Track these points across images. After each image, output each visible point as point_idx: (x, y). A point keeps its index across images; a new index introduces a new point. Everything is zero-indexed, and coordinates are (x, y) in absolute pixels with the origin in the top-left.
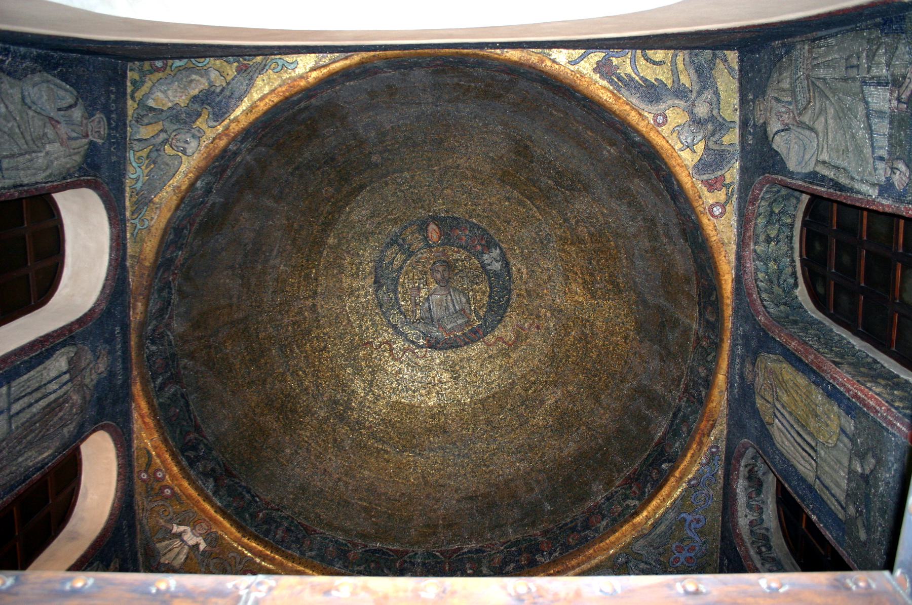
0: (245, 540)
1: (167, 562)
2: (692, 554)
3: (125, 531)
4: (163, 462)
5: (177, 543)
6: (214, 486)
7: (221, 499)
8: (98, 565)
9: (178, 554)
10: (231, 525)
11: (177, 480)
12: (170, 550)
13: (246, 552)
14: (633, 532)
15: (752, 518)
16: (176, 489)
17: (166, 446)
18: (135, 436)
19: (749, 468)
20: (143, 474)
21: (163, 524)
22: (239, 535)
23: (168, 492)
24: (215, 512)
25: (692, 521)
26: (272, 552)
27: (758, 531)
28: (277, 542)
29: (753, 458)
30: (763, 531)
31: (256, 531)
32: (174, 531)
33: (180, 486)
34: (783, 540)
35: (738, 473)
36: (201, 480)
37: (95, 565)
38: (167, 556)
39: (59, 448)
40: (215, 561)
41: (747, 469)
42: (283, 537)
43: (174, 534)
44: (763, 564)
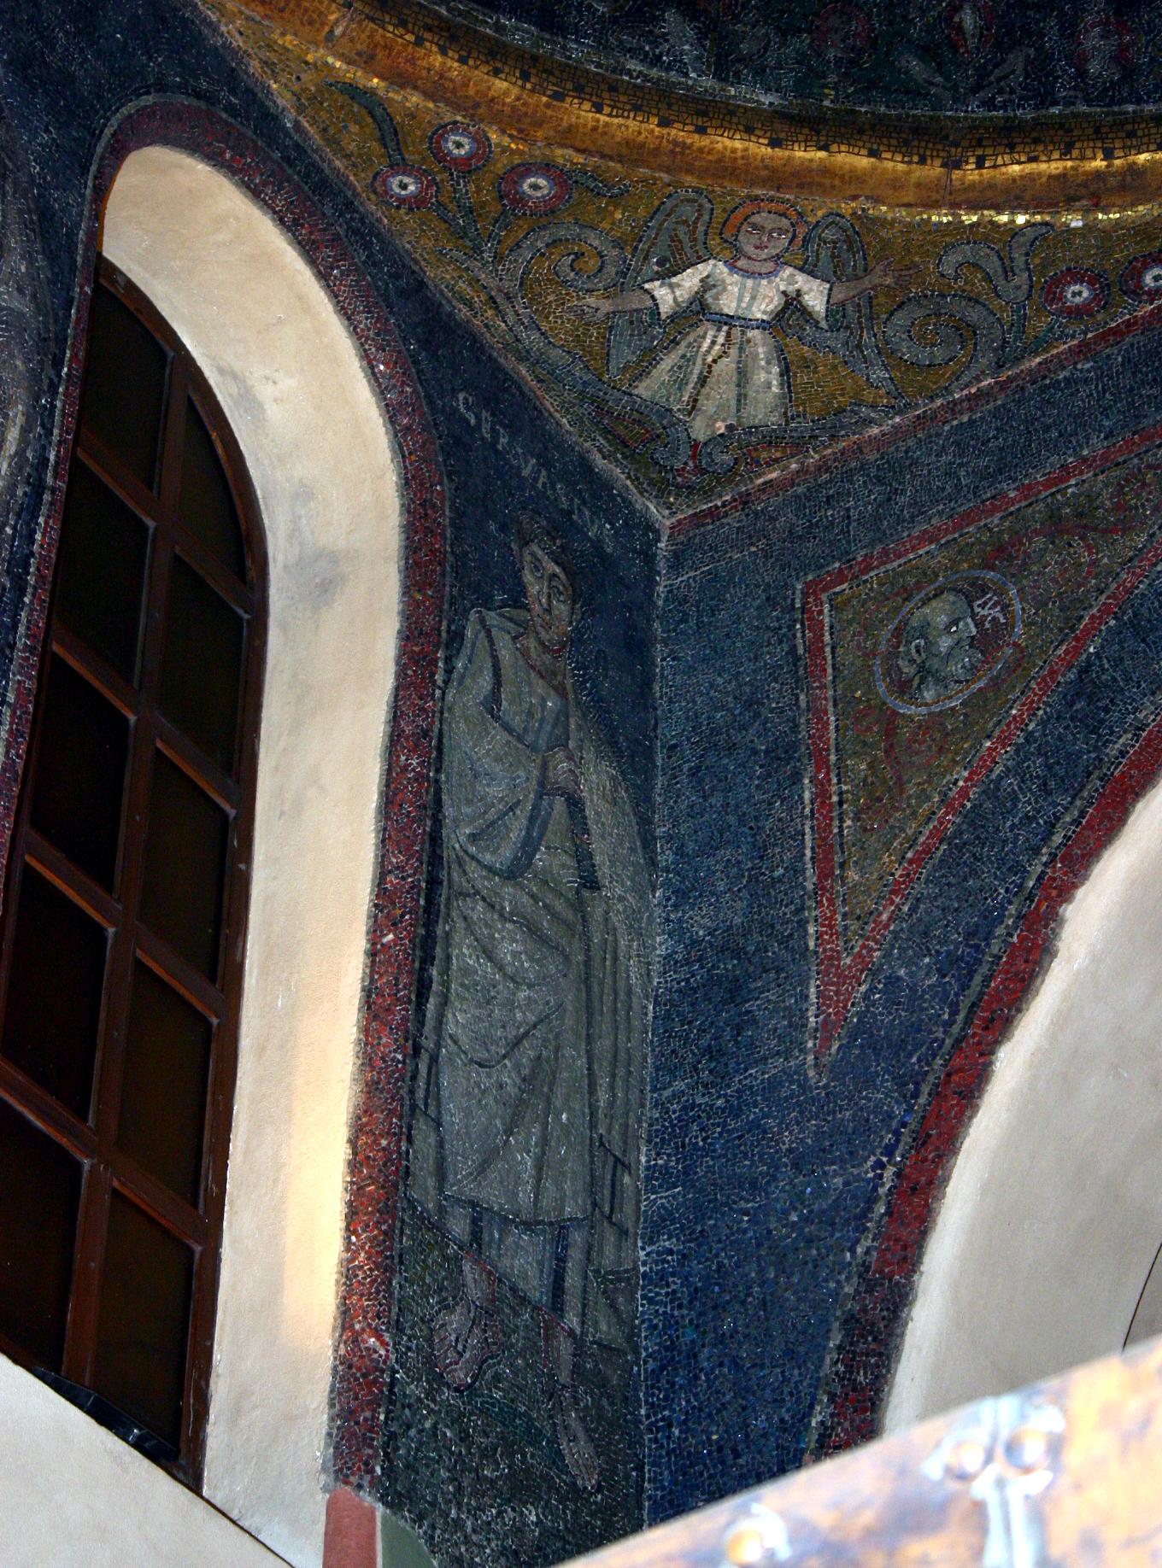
0: (970, 174)
1: (721, 427)
3: (485, 431)
4: (437, 90)
5: (710, 340)
6: (702, 35)
7: (760, 72)
8: (482, 621)
9: (743, 375)
10: (872, 154)
11: (539, 124)
12: (703, 381)
13: (1004, 218)
16: (561, 155)
17: (402, 23)
18: (254, 66)
20: (394, 182)
21: (606, 306)
22: (933, 171)
23: (537, 186)
24: (774, 143)
26: (1108, 155)
28: (1108, 95)
31: (989, 104)
32: (666, 308)
33: (567, 136)
36: (633, 52)
37: (469, 633)
38: (708, 406)
39: (34, 377)
40: (900, 319)
42: (1120, 58)
43: (673, 317)
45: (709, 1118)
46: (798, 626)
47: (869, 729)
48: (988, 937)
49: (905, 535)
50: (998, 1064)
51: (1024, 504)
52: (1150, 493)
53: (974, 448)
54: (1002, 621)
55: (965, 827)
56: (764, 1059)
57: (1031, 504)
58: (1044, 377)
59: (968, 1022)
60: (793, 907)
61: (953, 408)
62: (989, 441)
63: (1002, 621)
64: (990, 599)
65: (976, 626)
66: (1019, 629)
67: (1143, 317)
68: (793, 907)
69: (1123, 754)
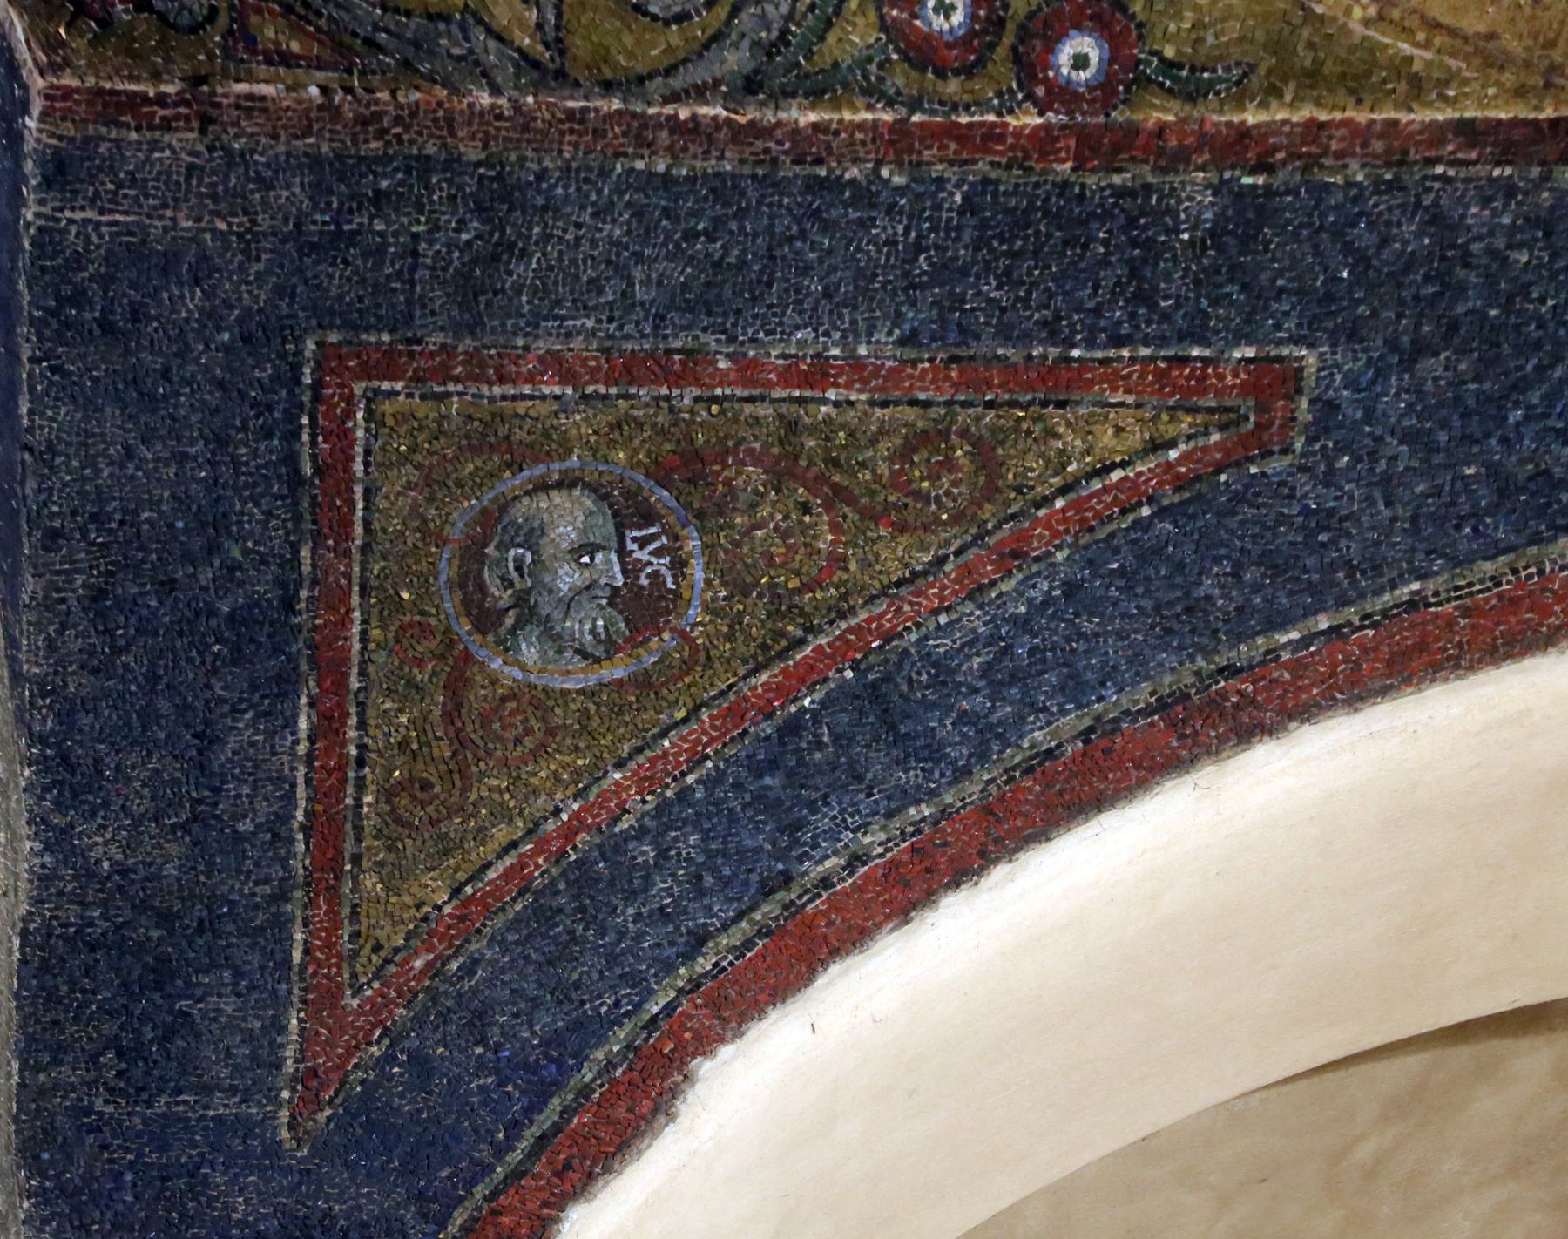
45: (114, 1137)
46: (305, 420)
47: (420, 663)
48: (580, 1057)
49: (520, 342)
50: (567, 1225)
51: (739, 392)
52: (955, 484)
53: (668, 238)
54: (671, 586)
55: (562, 886)
56: (207, 1089)
57: (751, 400)
58: (819, 161)
59: (533, 1154)
60: (267, 889)
61: (641, 133)
62: (697, 235)
63: (671, 586)
64: (653, 537)
65: (624, 572)
66: (695, 613)
67: (1018, 133)
68: (267, 889)
69: (825, 882)
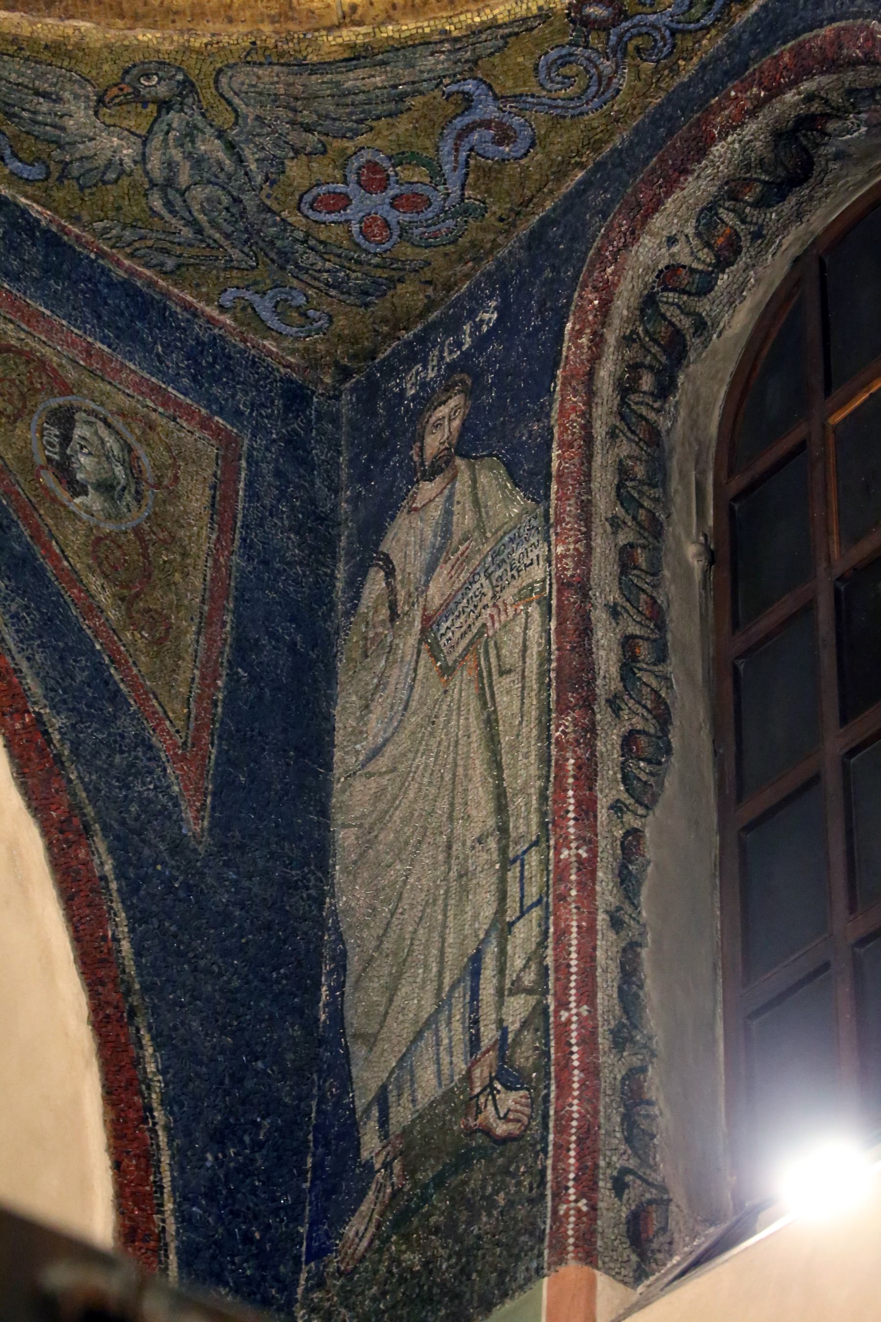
2: (394, 217)
14: (267, 28)
15: (685, 259)
19: (816, 107)
25: (486, 124)
27: (671, 312)
29: (850, 92)
30: (685, 323)
34: (725, 388)
35: (768, 100)
41: (803, 109)
44: (612, 434)
